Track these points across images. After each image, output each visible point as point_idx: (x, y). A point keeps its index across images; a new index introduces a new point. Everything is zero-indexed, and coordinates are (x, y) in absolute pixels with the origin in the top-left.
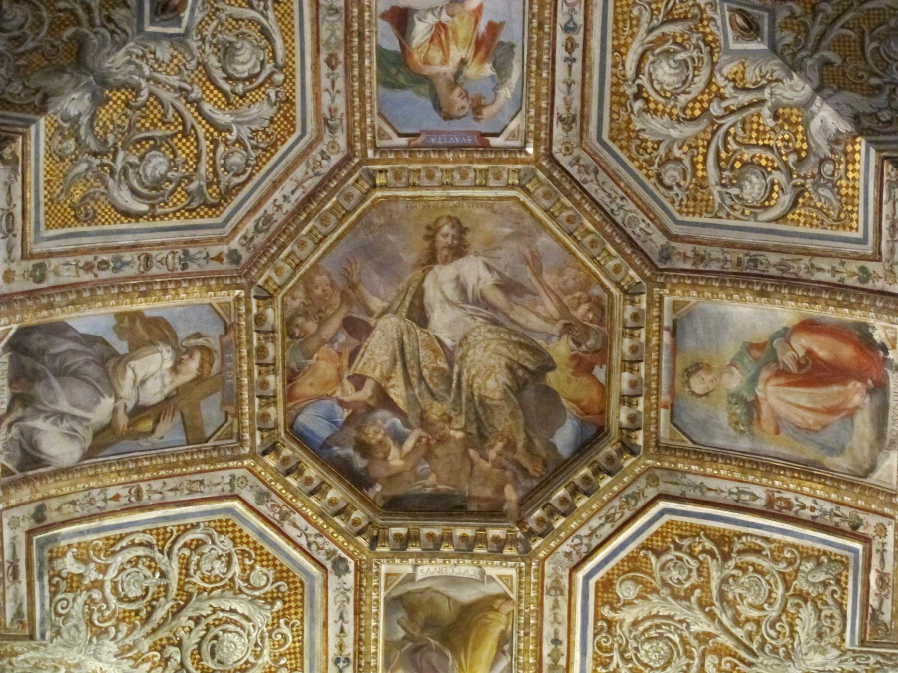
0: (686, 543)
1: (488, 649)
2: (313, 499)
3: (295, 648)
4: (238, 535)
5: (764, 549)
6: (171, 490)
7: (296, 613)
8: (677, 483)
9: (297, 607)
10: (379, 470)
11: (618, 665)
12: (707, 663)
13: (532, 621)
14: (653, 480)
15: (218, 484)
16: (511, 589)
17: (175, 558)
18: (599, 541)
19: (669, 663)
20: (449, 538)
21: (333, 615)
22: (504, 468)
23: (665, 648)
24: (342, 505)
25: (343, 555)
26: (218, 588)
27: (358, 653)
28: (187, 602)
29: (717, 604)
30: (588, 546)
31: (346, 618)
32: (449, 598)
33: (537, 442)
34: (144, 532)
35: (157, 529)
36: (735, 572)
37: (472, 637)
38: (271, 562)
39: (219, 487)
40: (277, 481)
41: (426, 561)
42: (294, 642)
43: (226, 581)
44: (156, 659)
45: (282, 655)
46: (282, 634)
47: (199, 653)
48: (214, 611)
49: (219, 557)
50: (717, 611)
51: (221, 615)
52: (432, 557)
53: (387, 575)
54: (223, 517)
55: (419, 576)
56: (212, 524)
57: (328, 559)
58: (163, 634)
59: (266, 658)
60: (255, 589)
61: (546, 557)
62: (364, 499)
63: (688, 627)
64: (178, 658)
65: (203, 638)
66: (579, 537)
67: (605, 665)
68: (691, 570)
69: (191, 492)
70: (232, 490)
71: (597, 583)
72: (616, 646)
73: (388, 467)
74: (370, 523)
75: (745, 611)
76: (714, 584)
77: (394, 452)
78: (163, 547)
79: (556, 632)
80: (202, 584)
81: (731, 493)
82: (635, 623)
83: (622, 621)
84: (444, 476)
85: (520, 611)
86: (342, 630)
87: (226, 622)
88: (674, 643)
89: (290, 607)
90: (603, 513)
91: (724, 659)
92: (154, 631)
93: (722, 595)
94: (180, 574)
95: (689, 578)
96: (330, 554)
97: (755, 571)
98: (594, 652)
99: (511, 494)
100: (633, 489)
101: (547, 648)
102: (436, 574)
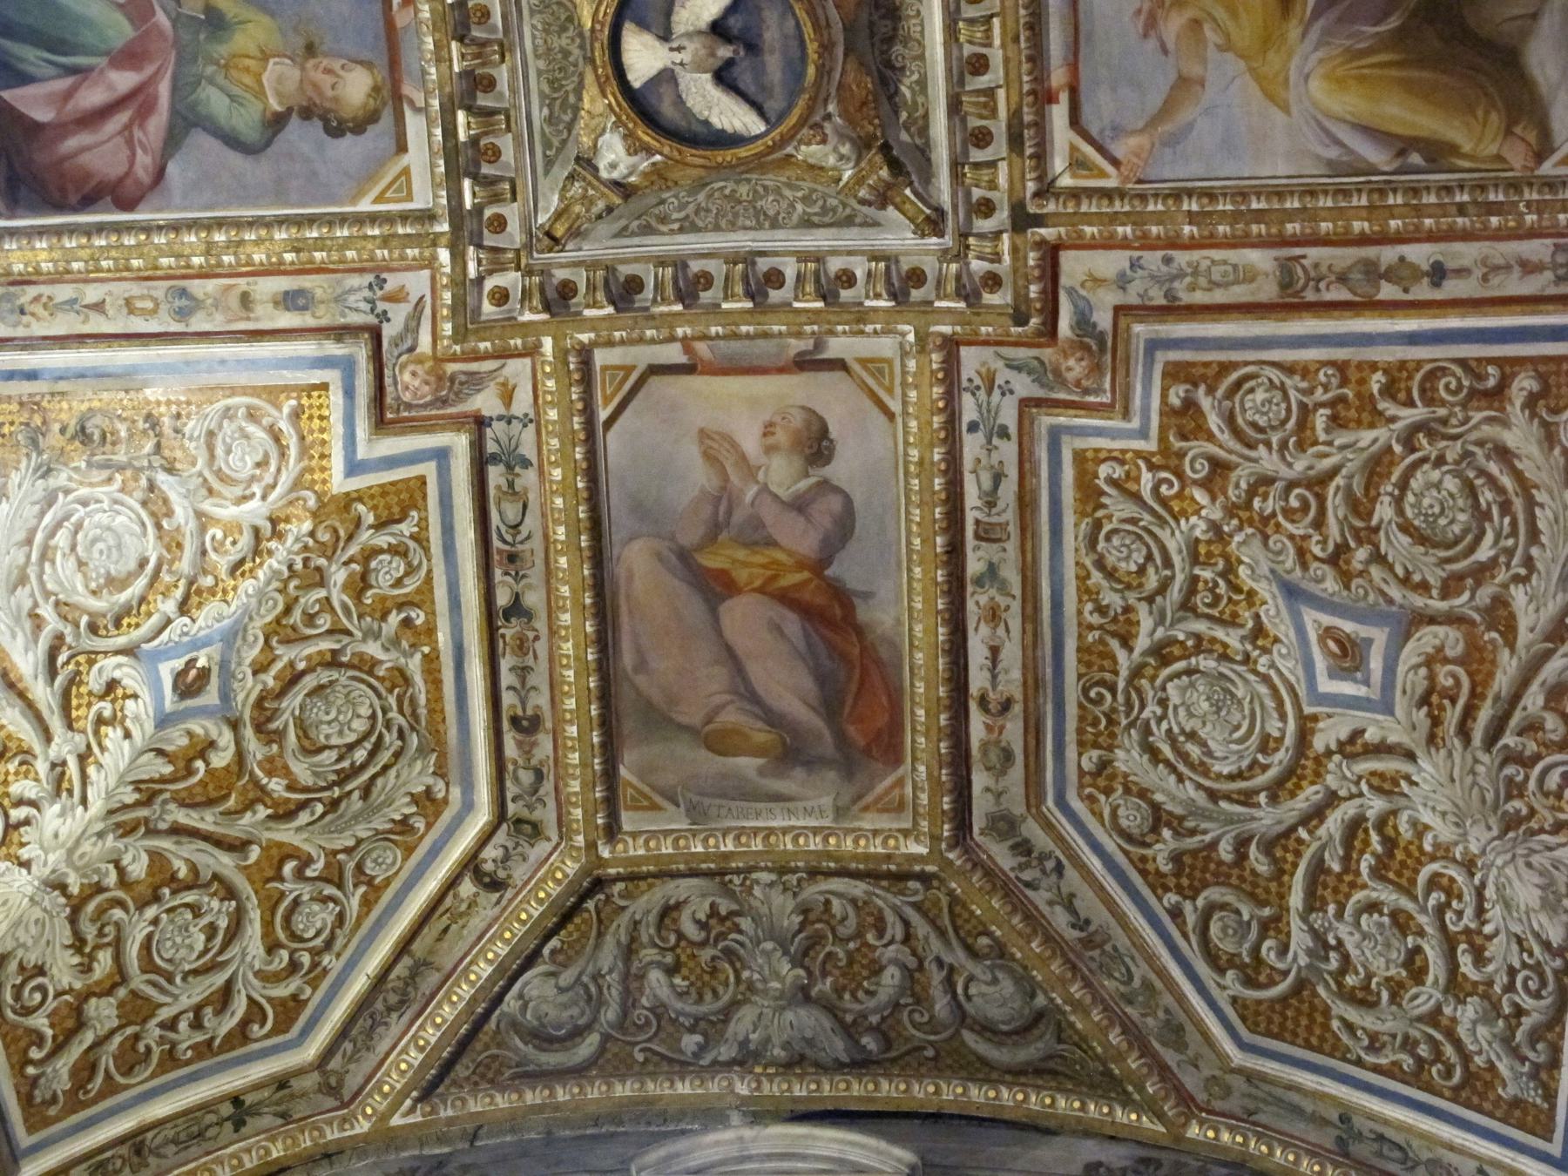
1: (1408, 116)
11: (1393, 419)
12: (1441, 630)
13: (1494, 220)
19: (1421, 539)
23: (1457, 529)
32: (1535, 16)
63: (1517, 579)
67: (1389, 391)
72: (1442, 412)
79: (1462, 272)
82: (1503, 454)
83: (1505, 424)
88: (1472, 549)
91: (1460, 671)
98: (1419, 364)
101: (1420, 254)
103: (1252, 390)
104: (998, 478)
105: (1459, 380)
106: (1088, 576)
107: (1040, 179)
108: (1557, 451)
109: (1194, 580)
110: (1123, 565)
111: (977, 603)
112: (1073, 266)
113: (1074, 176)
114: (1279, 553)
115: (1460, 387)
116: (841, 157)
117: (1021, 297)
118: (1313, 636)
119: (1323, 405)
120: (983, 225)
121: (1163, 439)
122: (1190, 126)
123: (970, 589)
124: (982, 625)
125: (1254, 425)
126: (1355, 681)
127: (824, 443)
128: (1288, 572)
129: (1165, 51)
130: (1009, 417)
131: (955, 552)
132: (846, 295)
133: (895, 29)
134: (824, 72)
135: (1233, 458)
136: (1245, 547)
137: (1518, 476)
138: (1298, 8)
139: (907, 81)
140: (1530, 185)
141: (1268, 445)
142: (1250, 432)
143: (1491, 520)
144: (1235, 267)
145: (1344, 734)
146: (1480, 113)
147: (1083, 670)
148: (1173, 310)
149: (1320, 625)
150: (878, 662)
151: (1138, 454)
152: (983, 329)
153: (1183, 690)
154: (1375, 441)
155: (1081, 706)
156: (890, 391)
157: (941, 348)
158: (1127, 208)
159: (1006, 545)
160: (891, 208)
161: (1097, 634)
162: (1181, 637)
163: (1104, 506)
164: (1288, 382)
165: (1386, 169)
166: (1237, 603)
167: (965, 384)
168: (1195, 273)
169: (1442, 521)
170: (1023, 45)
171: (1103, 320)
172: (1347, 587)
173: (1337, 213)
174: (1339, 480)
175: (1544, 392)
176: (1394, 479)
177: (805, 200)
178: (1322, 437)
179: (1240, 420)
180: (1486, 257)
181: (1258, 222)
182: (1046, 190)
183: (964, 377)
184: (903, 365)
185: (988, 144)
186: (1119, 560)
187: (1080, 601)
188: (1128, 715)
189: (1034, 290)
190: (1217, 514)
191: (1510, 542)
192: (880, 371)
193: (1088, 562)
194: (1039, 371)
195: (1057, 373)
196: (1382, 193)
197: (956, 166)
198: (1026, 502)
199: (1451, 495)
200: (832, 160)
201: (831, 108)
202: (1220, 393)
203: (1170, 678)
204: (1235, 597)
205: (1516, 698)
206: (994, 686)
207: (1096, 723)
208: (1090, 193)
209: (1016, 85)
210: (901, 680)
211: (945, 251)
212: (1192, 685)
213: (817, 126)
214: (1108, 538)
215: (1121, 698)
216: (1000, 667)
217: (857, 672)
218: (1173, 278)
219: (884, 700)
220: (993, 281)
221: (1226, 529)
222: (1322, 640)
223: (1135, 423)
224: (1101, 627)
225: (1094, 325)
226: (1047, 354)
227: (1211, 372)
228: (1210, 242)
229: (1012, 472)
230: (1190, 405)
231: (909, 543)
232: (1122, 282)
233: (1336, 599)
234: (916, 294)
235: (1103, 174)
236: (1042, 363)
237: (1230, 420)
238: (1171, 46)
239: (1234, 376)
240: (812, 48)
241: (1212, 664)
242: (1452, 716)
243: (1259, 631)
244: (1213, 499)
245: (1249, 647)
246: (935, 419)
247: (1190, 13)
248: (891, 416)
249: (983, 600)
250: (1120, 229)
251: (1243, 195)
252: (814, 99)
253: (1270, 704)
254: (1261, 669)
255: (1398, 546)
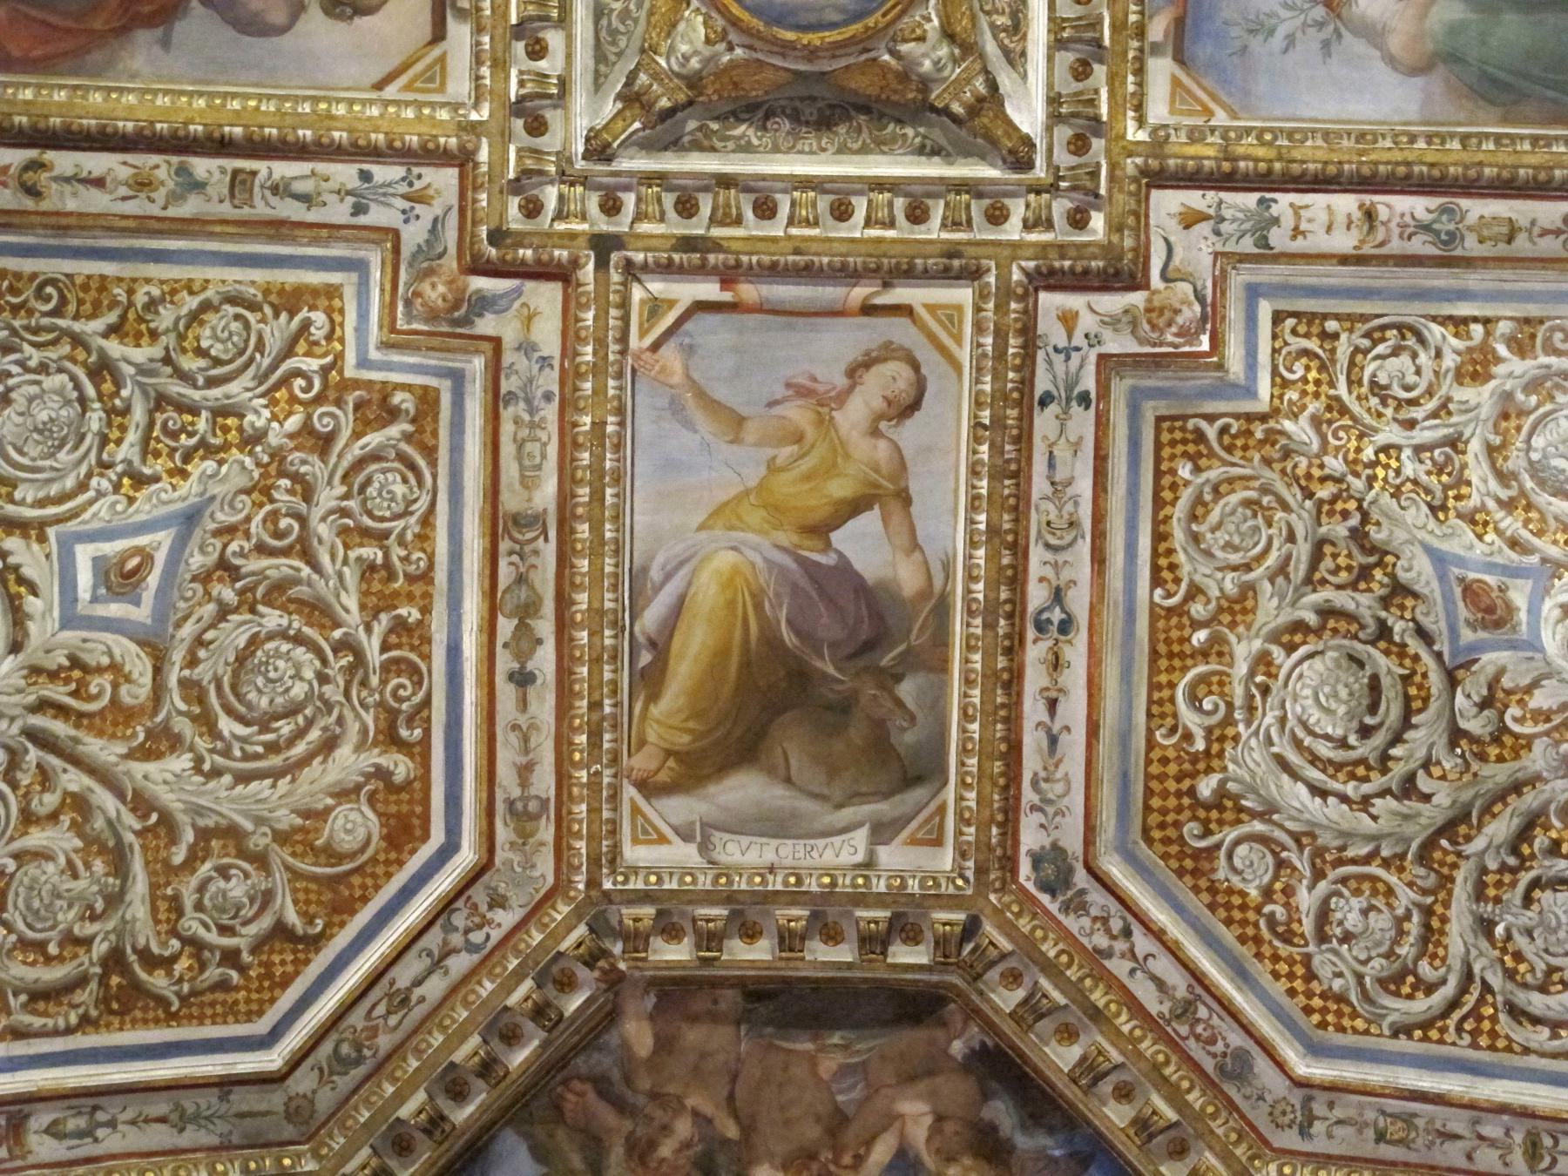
0: (213, 973)
2: (1116, 1056)
3: (1170, 669)
4: (1298, 985)
5: (26, 1007)
6: (1457, 1137)
7: (1164, 761)
8: (242, 1115)
9: (1162, 778)
10: (956, 1090)
11: (369, 629)
12: (147, 680)
13: (582, 739)
14: (299, 1112)
15: (1339, 1122)
16: (635, 810)
17: (1457, 965)
18: (425, 942)
19: (242, 658)
20: (789, 941)
21: (1076, 743)
22: (655, 1096)
23: (252, 696)
24: (1046, 1025)
25: (1045, 898)
26: (1354, 861)
27: (1014, 647)
28: (1429, 845)
29: (129, 837)
30: (449, 928)
31: (1042, 735)
32: (788, 780)
33: (577, 1162)
34: (1527, 1051)
35: (1492, 1048)
36: (90, 929)
37: (727, 690)
38: (1222, 900)
39: (1338, 1113)
40: (1200, 1116)
41: (844, 884)
42: (1172, 685)
43: (1332, 875)
44: (1514, 711)
45: (1204, 654)
46: (1200, 710)
47: (1407, 699)
48: (1366, 801)
49: (1347, 938)
50: (130, 820)
51: (1350, 789)
52: (829, 895)
53: (938, 842)
54: (1332, 1037)
55: (861, 837)
56: (1360, 1024)
57: (1082, 892)
58: (1497, 774)
59: (1243, 650)
60: (1263, 840)
61: (550, 896)
62: (989, 1026)
63: (199, 760)
64: (1460, 699)
65: (1397, 739)
66: (471, 948)
67: (400, 625)
68: (199, 907)
69: (1408, 1119)
70: (1308, 1100)
71: (426, 836)
72: (375, 680)
73: (932, 1096)
74: (978, 977)
75: (60, 839)
76: (140, 885)
77: (919, 1133)
78: (1481, 1001)
79: (523, 704)
80: (1393, 879)
81: (112, 1124)
82: (329, 745)
83: (359, 748)
84: (799, 1071)
85: (615, 760)
86: (1052, 705)
87: (1339, 766)
88: (230, 711)
89: (1179, 780)
90: (418, 1013)
91: (105, 700)
92: (1517, 788)
93: (119, 862)
94: (1444, 920)
95: (202, 889)
96: (1077, 905)
97: (41, 946)
98: (427, 657)
99: (638, 1033)
100: (344, 1083)
101: (545, 660)
102: (821, 842)
103: (405, 481)
104: (306, 199)
105: (408, 699)
106: (191, 293)
107: (645, 267)
108: (330, 801)
109: (194, 411)
110: (208, 332)
111: (157, 167)
112: (546, 297)
113: (643, 302)
114: (232, 506)
115: (401, 700)
116: (686, 58)
117: (520, 239)
118: (142, 540)
119: (386, 556)
120: (593, 202)
121: (356, 384)
122: (689, 425)
123: (175, 159)
124: (132, 171)
125: (368, 482)
126: (95, 587)
127: (349, 11)
128: (212, 516)
129: (773, 404)
130: (377, 216)
131: (220, 146)
132: (519, 47)
133: (807, 123)
134: (786, 48)
135: (333, 459)
136: (239, 467)
137: (305, 761)
138: (807, 543)
139: (751, 132)
140: (615, 776)
141: (346, 497)
142: (361, 478)
143: (260, 732)
144: (539, 467)
145: (27, 571)
146: (691, 724)
147: (78, 281)
148: (496, 401)
149: (157, 549)
150: (79, 52)
151: (340, 356)
152: (484, 196)
153: (60, 392)
154: (347, 611)
155: (34, 276)
156: (408, 87)
157: (462, 147)
158: (611, 357)
159: (227, 204)
160: (619, 105)
161: (123, 298)
162: (125, 393)
163: (277, 315)
164: (413, 520)
165: (637, 629)
166: (171, 456)
167: (416, 170)
168: (533, 426)
169: (260, 681)
170: (791, 258)
171: (486, 325)
172: (194, 579)
173: (597, 574)
174: (306, 571)
175: (392, 788)
176: (306, 630)
177: (625, 14)
178: (352, 555)
179: (374, 467)
180: (538, 729)
181: (591, 495)
182: (632, 271)
183: (423, 170)
184: (443, 105)
185: (679, 213)
186: (213, 329)
187: (162, 282)
188: (27, 328)
189: (527, 253)
190: (274, 439)
191: (238, 753)
192: (431, 80)
193: (209, 293)
194: (429, 253)
195: (430, 272)
196: (614, 624)
197: (660, 178)
198: (278, 228)
199: (287, 690)
200: (684, 48)
201: (739, 51)
202: (404, 446)
203: (73, 378)
204: (177, 456)
205: (76, 761)
206: (56, 179)
207: (13, 291)
208: (625, 319)
209: (748, 248)
210: (61, 74)
211: (570, 161)
212: (67, 403)
213: (723, 36)
214: (237, 317)
215: (45, 321)
216: (80, 187)
217: (70, 24)
218: (528, 401)
219: (37, 53)
220: (532, 209)
221: (258, 449)
222: (138, 551)
223: (374, 354)
224: (131, 304)
225: (480, 315)
226: (451, 263)
227: (431, 443)
228: (569, 443)
229: (312, 216)
230: (393, 414)
231: (234, 96)
232: (527, 347)
233: (182, 566)
234: (518, 124)
235: (643, 333)
236: (440, 256)
237: (375, 457)
238: (777, 410)
239: (422, 463)
240: (814, 38)
241: (95, 426)
242: (58, 693)
243: (140, 481)
244: (291, 436)
245: (119, 468)
246: (381, 137)
247: (810, 433)
248: (379, 86)
249: (162, 173)
250: (589, 349)
251: (617, 480)
252: (758, 35)
253: (54, 490)
254: (94, 482)
255: (235, 632)
